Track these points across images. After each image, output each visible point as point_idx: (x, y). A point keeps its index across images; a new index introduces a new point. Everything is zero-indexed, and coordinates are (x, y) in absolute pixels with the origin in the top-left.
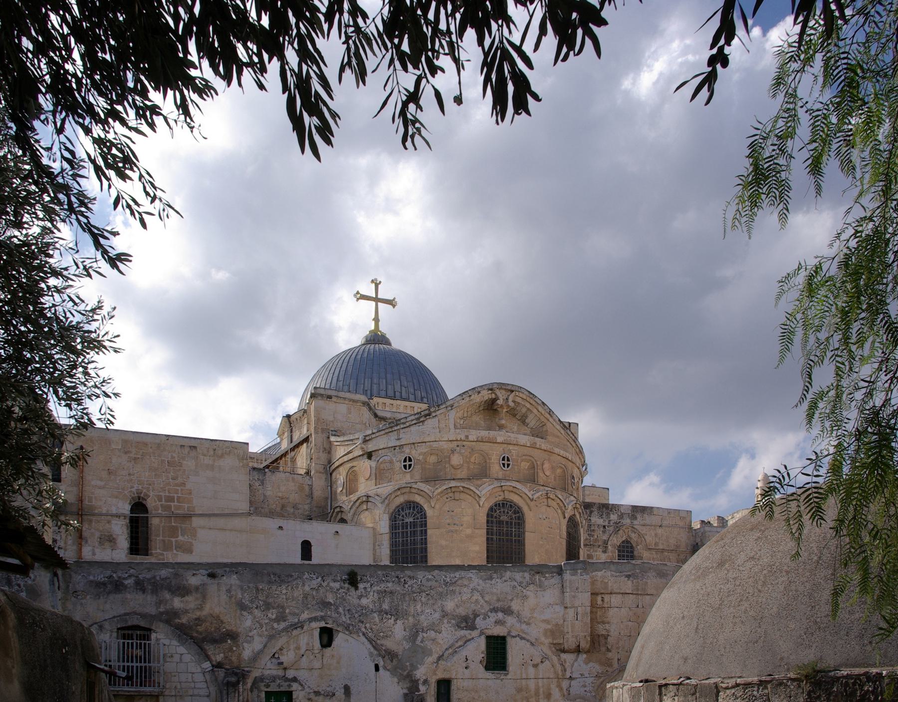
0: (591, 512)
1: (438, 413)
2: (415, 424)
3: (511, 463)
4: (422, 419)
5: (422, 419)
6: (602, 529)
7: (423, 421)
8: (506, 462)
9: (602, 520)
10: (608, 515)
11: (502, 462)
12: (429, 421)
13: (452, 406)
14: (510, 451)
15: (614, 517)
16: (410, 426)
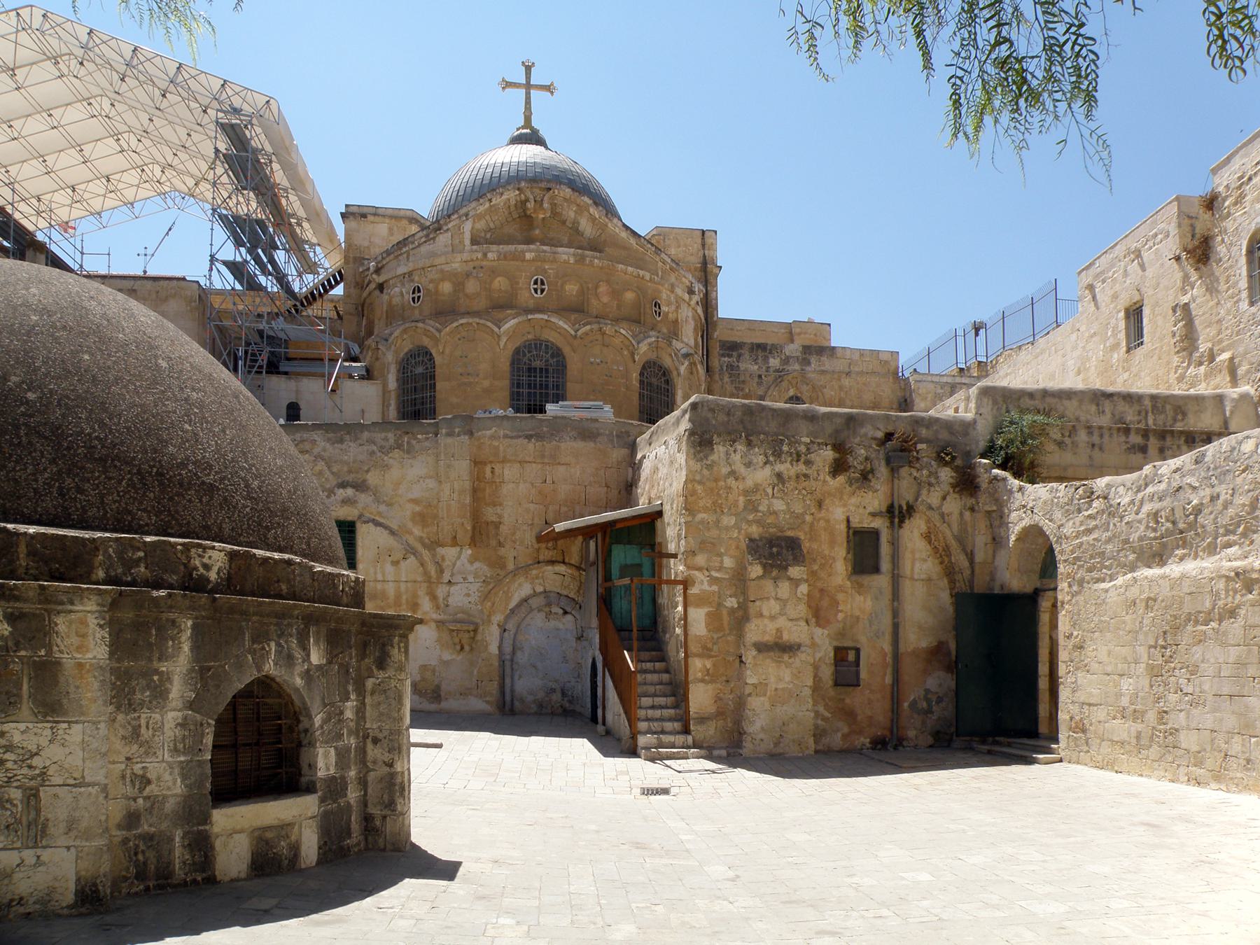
0: (740, 356)
1: (450, 226)
2: (425, 242)
3: (546, 287)
4: (431, 236)
5: (431, 236)
6: (756, 379)
7: (434, 239)
8: (539, 286)
9: (756, 367)
10: (766, 359)
11: (533, 286)
12: (441, 236)
13: (467, 215)
14: (544, 272)
15: (774, 362)
16: (420, 245)
